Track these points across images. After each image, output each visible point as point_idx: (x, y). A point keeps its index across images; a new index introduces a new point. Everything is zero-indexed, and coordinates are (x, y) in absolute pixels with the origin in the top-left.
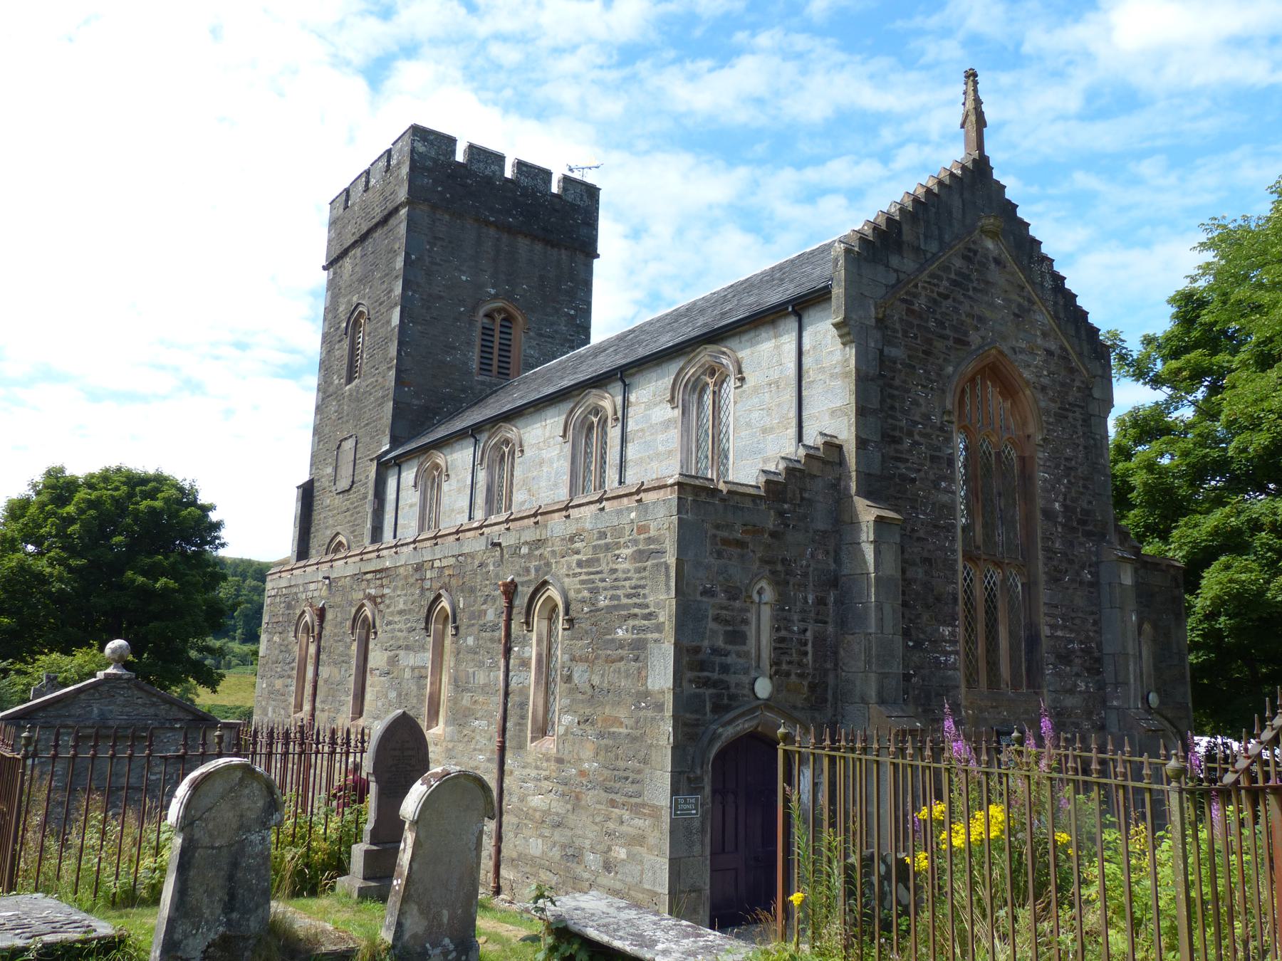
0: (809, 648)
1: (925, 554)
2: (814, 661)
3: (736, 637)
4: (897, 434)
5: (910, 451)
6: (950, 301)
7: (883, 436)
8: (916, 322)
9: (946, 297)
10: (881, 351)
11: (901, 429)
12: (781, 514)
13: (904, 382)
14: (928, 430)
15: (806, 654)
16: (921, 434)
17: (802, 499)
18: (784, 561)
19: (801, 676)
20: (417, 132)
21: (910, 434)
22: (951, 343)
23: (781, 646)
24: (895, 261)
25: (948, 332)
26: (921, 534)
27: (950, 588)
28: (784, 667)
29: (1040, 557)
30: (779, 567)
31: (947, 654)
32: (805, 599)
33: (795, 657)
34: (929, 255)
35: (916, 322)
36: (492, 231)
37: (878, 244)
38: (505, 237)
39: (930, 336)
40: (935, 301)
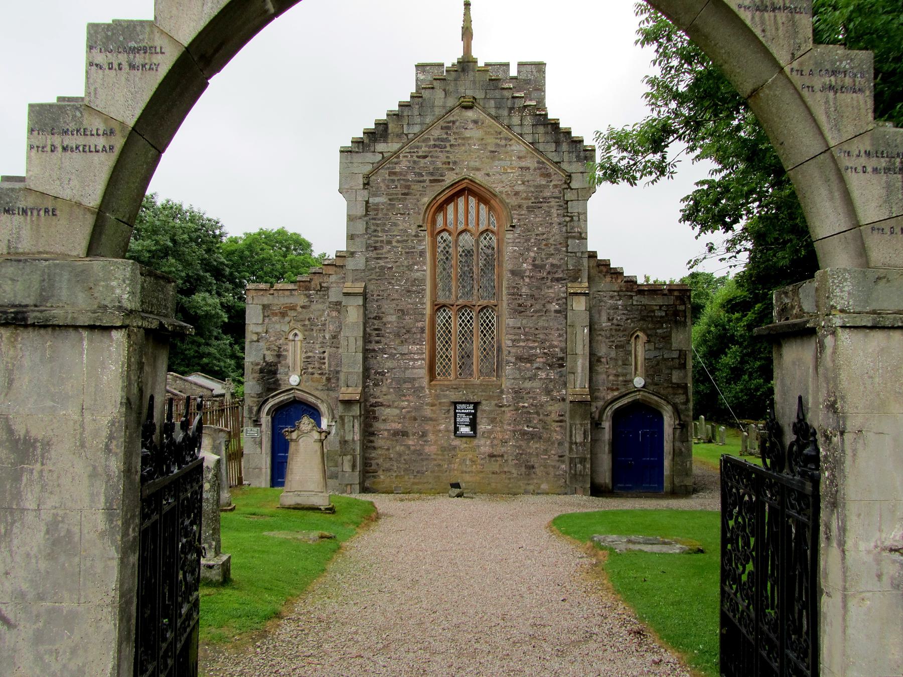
2: (330, 366)
4: (378, 245)
5: (389, 252)
6: (428, 159)
7: (367, 248)
8: (396, 178)
9: (425, 157)
10: (367, 202)
11: (382, 241)
12: (308, 296)
13: (386, 214)
14: (405, 238)
15: (324, 363)
17: (321, 287)
19: (321, 374)
20: (421, 67)
22: (428, 183)
23: (308, 360)
24: (381, 147)
26: (396, 296)
27: (420, 324)
28: (310, 370)
29: (504, 298)
30: (307, 322)
33: (317, 365)
34: (410, 136)
35: (396, 178)
37: (366, 141)
39: (409, 183)
40: (415, 162)
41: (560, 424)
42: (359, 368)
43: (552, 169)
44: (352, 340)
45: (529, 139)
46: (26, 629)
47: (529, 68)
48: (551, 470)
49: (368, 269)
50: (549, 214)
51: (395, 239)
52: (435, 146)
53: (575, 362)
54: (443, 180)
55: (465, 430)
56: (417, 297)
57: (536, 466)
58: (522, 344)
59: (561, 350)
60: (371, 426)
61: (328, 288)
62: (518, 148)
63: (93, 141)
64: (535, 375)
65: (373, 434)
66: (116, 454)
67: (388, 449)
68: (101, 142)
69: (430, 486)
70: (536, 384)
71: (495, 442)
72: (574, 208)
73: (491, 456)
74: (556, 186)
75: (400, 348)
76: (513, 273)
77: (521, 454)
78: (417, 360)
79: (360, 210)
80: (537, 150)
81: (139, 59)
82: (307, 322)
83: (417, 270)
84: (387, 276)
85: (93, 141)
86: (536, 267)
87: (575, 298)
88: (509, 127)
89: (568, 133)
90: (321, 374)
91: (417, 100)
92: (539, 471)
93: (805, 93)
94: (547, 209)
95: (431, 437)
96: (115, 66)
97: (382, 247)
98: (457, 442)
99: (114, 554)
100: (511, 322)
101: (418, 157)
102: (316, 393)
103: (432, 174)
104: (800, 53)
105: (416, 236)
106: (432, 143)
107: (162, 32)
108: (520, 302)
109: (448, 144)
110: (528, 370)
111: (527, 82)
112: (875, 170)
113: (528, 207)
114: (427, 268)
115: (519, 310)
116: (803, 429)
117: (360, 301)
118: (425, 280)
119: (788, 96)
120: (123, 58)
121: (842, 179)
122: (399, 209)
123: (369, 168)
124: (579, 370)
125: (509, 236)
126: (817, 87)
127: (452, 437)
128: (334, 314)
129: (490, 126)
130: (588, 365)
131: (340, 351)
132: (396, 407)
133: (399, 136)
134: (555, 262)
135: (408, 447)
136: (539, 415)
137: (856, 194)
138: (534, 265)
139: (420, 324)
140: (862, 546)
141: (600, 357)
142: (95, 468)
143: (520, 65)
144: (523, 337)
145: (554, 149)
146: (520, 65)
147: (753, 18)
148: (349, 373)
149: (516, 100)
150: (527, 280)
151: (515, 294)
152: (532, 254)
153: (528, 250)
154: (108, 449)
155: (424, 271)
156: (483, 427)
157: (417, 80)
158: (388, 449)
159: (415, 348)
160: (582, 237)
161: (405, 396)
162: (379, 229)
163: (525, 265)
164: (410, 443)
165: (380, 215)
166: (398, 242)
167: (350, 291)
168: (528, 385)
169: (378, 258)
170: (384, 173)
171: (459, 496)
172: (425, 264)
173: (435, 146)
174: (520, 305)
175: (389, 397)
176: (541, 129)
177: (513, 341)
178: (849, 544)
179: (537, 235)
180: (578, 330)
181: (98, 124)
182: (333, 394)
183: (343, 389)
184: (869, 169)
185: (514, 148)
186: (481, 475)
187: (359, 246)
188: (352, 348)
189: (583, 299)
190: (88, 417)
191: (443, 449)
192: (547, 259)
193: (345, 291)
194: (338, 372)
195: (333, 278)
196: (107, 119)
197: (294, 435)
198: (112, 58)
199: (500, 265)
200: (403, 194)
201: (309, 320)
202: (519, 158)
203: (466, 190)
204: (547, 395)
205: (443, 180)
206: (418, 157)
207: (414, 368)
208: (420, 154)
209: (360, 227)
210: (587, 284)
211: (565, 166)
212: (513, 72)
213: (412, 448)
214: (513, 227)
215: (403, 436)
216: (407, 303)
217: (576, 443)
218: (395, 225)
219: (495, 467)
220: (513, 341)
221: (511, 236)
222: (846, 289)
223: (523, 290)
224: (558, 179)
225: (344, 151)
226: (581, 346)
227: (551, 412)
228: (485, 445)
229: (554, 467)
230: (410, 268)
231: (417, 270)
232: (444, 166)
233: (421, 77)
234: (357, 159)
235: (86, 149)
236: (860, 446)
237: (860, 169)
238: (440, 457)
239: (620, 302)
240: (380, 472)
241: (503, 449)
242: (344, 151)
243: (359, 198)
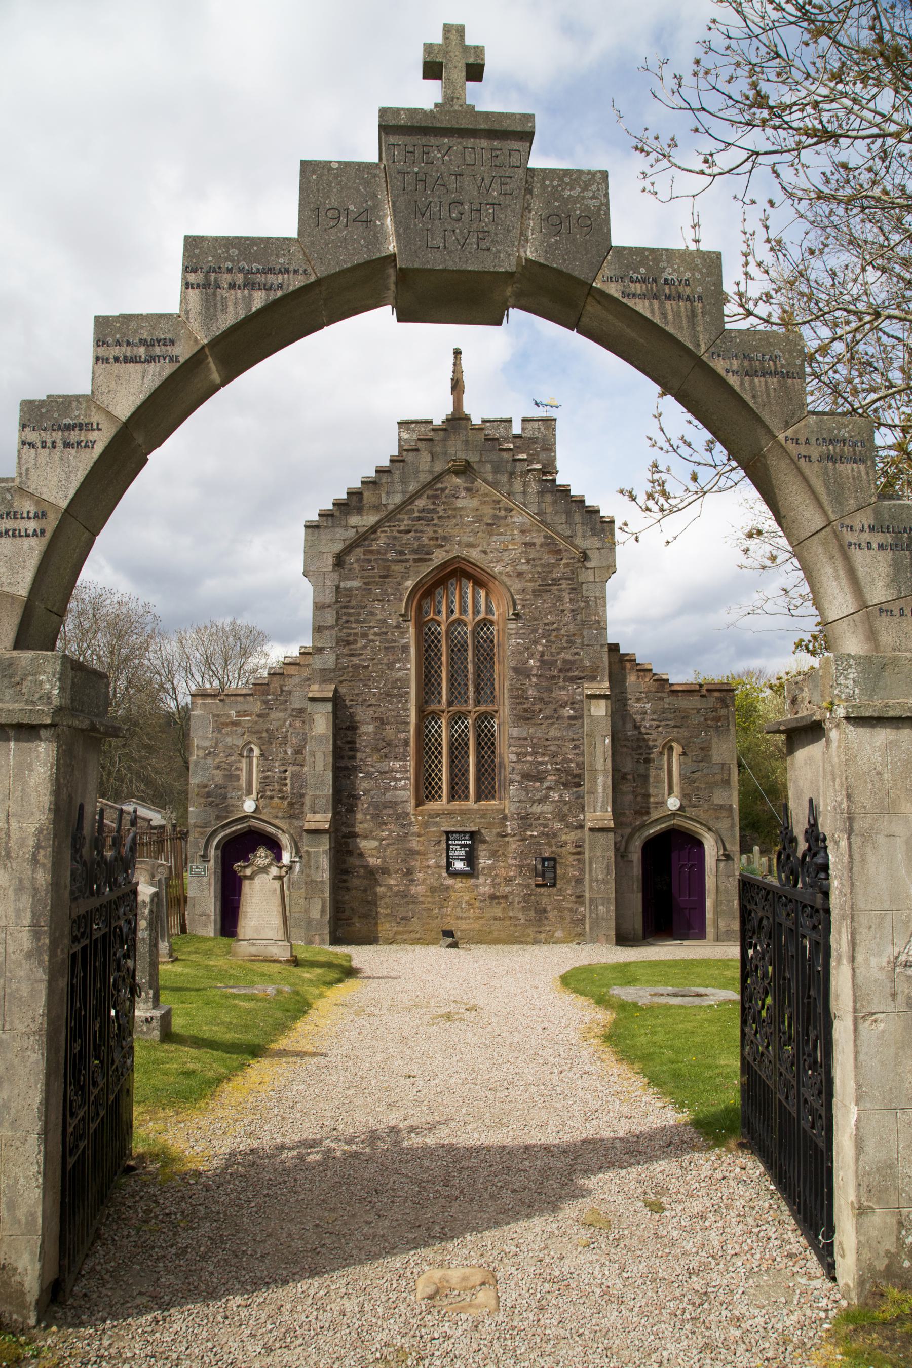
0: (288, 781)
1: (377, 715)
2: (292, 789)
3: (232, 777)
4: (351, 638)
5: (364, 647)
7: (337, 643)
8: (373, 558)
9: (408, 532)
10: (338, 587)
11: (355, 634)
12: (266, 702)
14: (384, 630)
15: (286, 785)
16: (376, 634)
17: (282, 691)
18: (267, 731)
21: (364, 636)
22: (411, 563)
23: (266, 782)
24: (354, 520)
25: (408, 557)
26: (373, 701)
27: (403, 735)
28: (269, 794)
29: (506, 702)
30: (264, 735)
31: (397, 780)
32: (286, 752)
33: (277, 787)
37: (337, 514)
40: (395, 538)
41: (576, 857)
42: (328, 790)
44: (319, 755)
47: (536, 424)
48: (567, 914)
49: (339, 669)
50: (560, 599)
51: (372, 631)
52: (419, 519)
53: (595, 780)
54: (430, 560)
55: (459, 865)
56: (400, 702)
57: (549, 908)
58: (529, 758)
59: (577, 765)
60: (344, 862)
61: (290, 692)
63: (22, 525)
64: (547, 797)
65: (346, 872)
66: (44, 865)
67: (365, 891)
68: (32, 525)
69: (418, 936)
70: (548, 808)
71: (497, 880)
72: (589, 592)
73: (493, 897)
75: (378, 765)
76: (516, 670)
77: (530, 895)
78: (400, 780)
79: (329, 597)
81: (74, 436)
82: (264, 735)
83: (400, 669)
84: (361, 677)
85: (22, 525)
87: (594, 702)
89: (581, 501)
90: (282, 798)
91: (397, 464)
92: (552, 915)
93: (802, 463)
94: (557, 593)
95: (419, 876)
96: (49, 445)
97: (356, 641)
98: (450, 881)
99: (41, 975)
100: (515, 732)
101: (399, 532)
102: (276, 822)
103: (416, 552)
104: (794, 420)
105: (398, 627)
106: (416, 514)
107: (99, 408)
108: (526, 706)
109: (435, 516)
110: (536, 790)
111: (533, 440)
112: (881, 547)
113: (534, 591)
114: (412, 666)
115: (525, 717)
116: (814, 836)
117: (329, 707)
118: (409, 680)
119: (784, 465)
120: (58, 436)
121: (847, 558)
122: (376, 594)
123: (338, 547)
124: (600, 790)
125: (512, 626)
126: (815, 456)
127: (445, 874)
128: (298, 723)
129: (487, 495)
130: (610, 782)
131: (305, 769)
132: (374, 838)
133: (377, 508)
134: (569, 657)
135: (390, 887)
136: (551, 846)
137: (861, 573)
138: (542, 662)
139: (403, 735)
140: (874, 961)
141: (626, 774)
142: (21, 880)
143: (524, 420)
144: (530, 750)
145: (564, 521)
146: (524, 420)
147: (742, 383)
148: (316, 796)
149: (518, 463)
150: (534, 680)
151: (519, 697)
152: (540, 648)
153: (535, 642)
154: (34, 861)
155: (408, 669)
156: (483, 862)
157: (400, 439)
158: (365, 891)
159: (398, 764)
160: (601, 626)
161: (385, 824)
162: (352, 619)
163: (531, 661)
164: (393, 882)
165: (353, 603)
166: (376, 634)
167: (317, 695)
168: (537, 809)
169: (351, 655)
170: (359, 552)
171: (454, 945)
172: (409, 662)
173: (419, 519)
174: (526, 711)
175: (366, 825)
176: (549, 498)
177: (518, 754)
178: (860, 958)
179: (546, 624)
180: (598, 739)
181: (28, 506)
182: (296, 823)
183: (309, 816)
184: (875, 546)
185: (516, 520)
186: (481, 922)
188: (320, 766)
189: (603, 703)
190: (14, 825)
191: (433, 890)
192: (558, 653)
193: (310, 695)
194: (302, 796)
195: (296, 680)
196: (39, 501)
197: (248, 872)
198: (48, 437)
200: (380, 577)
201: (267, 731)
202: (523, 532)
203: (458, 572)
204: (560, 821)
205: (430, 560)
206: (399, 532)
207: (395, 788)
208: (402, 528)
209: (330, 618)
210: (607, 684)
211: (578, 541)
212: (517, 429)
213: (396, 888)
214: (517, 615)
215: (383, 873)
217: (597, 881)
218: (372, 614)
219: (498, 911)
220: (518, 754)
221: (514, 626)
222: (851, 676)
223: (530, 692)
225: (310, 527)
226: (602, 760)
227: (566, 843)
228: (484, 884)
229: (571, 910)
230: (390, 666)
231: (400, 669)
232: (432, 543)
233: (405, 436)
234: (325, 535)
235: (15, 534)
236: (868, 850)
237: (864, 544)
238: (429, 899)
239: (648, 706)
240: (356, 919)
241: (507, 889)
242: (310, 527)
243: (328, 583)
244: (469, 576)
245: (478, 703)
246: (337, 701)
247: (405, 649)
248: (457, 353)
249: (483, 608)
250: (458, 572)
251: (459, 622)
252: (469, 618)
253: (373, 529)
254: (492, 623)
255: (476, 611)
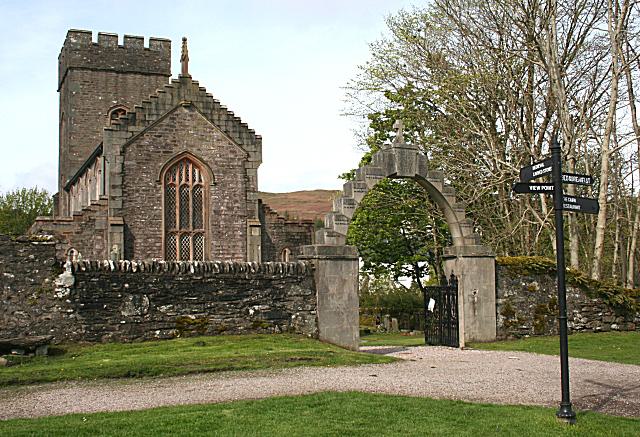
21: (137, 191)
24: (131, 128)
27: (158, 244)
36: (114, 74)
38: (120, 75)
43: (237, 148)
45: (224, 128)
46: (345, 314)
47: (158, 43)
62: (217, 134)
72: (250, 174)
74: (239, 159)
80: (228, 136)
86: (230, 209)
88: (212, 121)
89: (245, 126)
100: (214, 242)
105: (155, 187)
114: (162, 208)
115: (219, 235)
118: (161, 216)
123: (124, 142)
128: (99, 237)
133: (144, 121)
138: (227, 207)
139: (158, 244)
143: (151, 40)
146: (151, 40)
167: (115, 223)
170: (134, 145)
172: (160, 205)
176: (230, 123)
187: (118, 192)
195: (98, 214)
199: (207, 207)
203: (184, 160)
211: (245, 147)
216: (150, 230)
224: (241, 153)
244: (190, 162)
245: (194, 228)
246: (125, 225)
247: (159, 198)
248: (185, 40)
249: (197, 179)
250: (184, 160)
251: (185, 185)
252: (190, 183)
253: (142, 134)
254: (201, 186)
255: (194, 181)
